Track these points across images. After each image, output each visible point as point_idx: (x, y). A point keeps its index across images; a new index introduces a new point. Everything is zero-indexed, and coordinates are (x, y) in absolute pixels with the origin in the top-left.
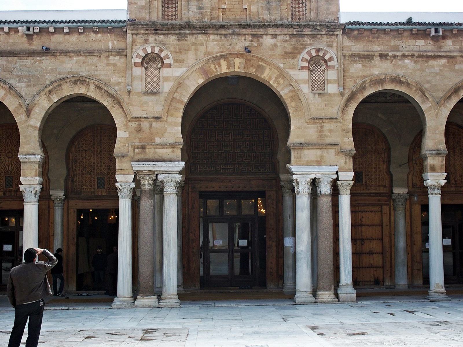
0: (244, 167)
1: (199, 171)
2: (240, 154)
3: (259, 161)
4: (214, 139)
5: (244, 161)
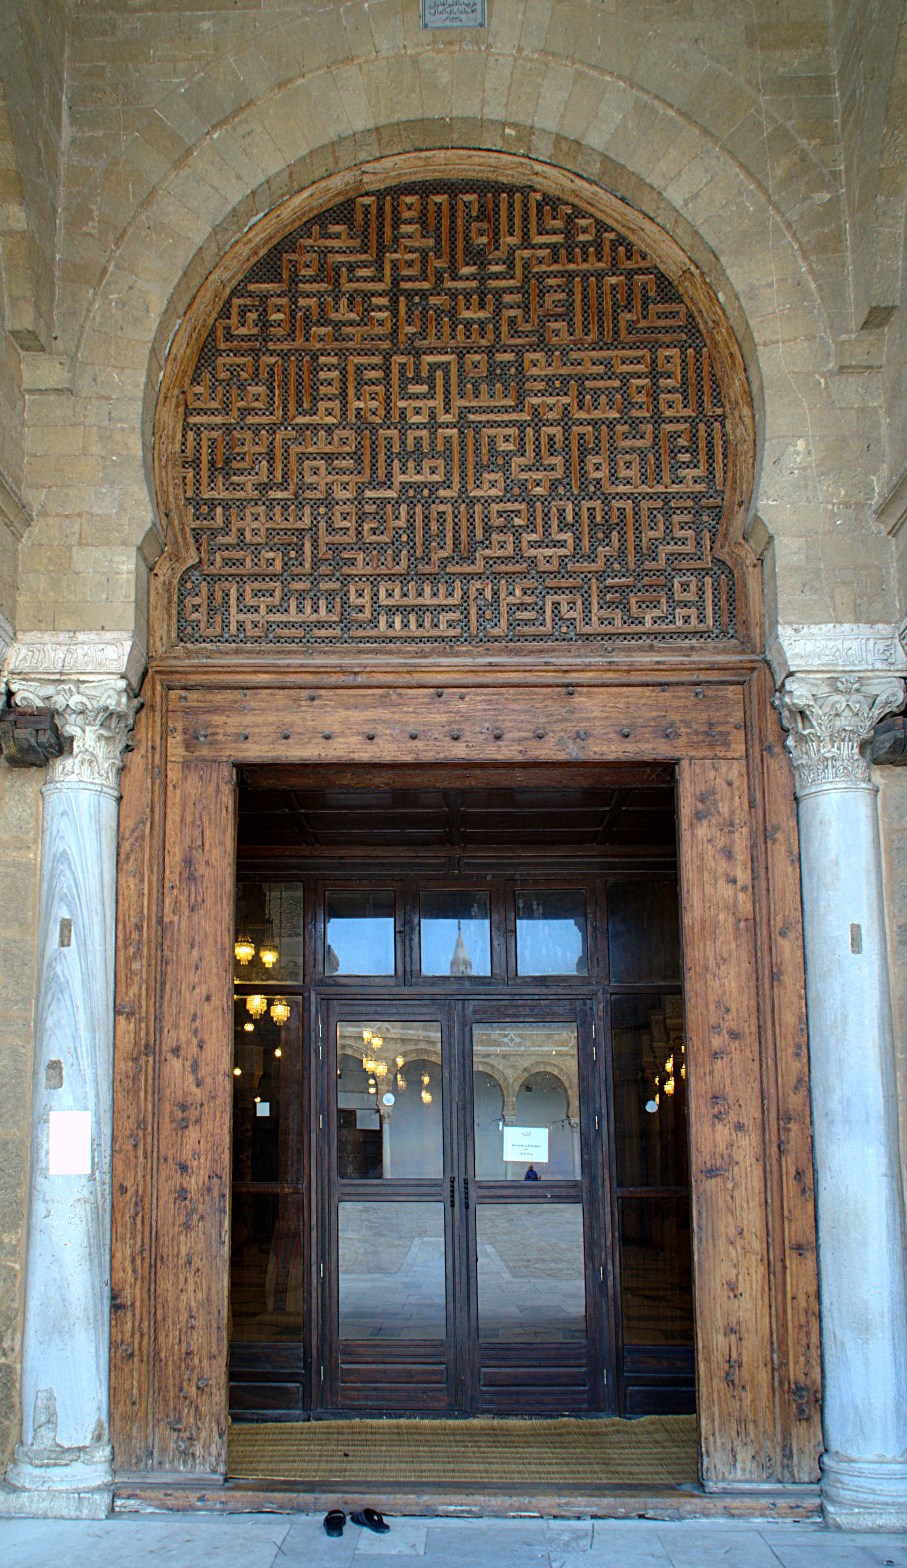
0: (527, 599)
1: (233, 627)
2: (501, 507)
3: (631, 559)
4: (337, 412)
5: (533, 560)
